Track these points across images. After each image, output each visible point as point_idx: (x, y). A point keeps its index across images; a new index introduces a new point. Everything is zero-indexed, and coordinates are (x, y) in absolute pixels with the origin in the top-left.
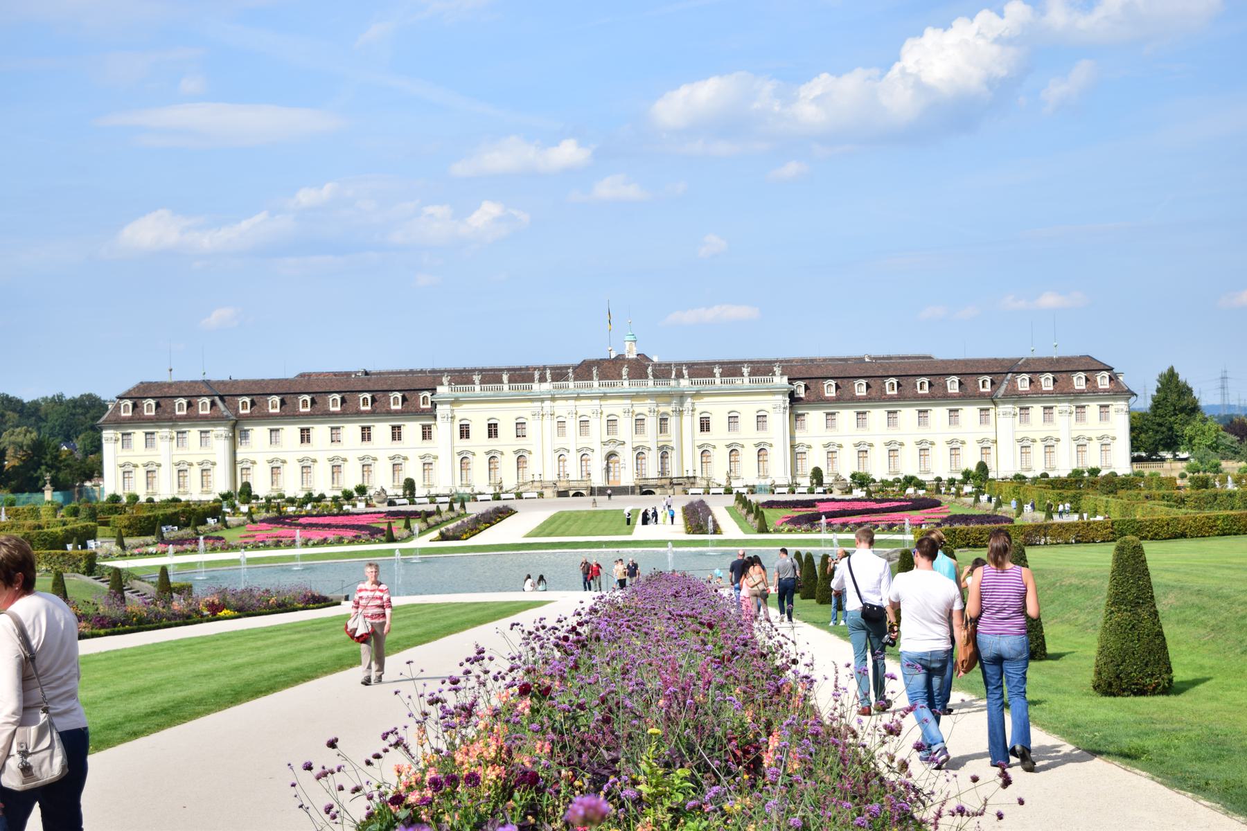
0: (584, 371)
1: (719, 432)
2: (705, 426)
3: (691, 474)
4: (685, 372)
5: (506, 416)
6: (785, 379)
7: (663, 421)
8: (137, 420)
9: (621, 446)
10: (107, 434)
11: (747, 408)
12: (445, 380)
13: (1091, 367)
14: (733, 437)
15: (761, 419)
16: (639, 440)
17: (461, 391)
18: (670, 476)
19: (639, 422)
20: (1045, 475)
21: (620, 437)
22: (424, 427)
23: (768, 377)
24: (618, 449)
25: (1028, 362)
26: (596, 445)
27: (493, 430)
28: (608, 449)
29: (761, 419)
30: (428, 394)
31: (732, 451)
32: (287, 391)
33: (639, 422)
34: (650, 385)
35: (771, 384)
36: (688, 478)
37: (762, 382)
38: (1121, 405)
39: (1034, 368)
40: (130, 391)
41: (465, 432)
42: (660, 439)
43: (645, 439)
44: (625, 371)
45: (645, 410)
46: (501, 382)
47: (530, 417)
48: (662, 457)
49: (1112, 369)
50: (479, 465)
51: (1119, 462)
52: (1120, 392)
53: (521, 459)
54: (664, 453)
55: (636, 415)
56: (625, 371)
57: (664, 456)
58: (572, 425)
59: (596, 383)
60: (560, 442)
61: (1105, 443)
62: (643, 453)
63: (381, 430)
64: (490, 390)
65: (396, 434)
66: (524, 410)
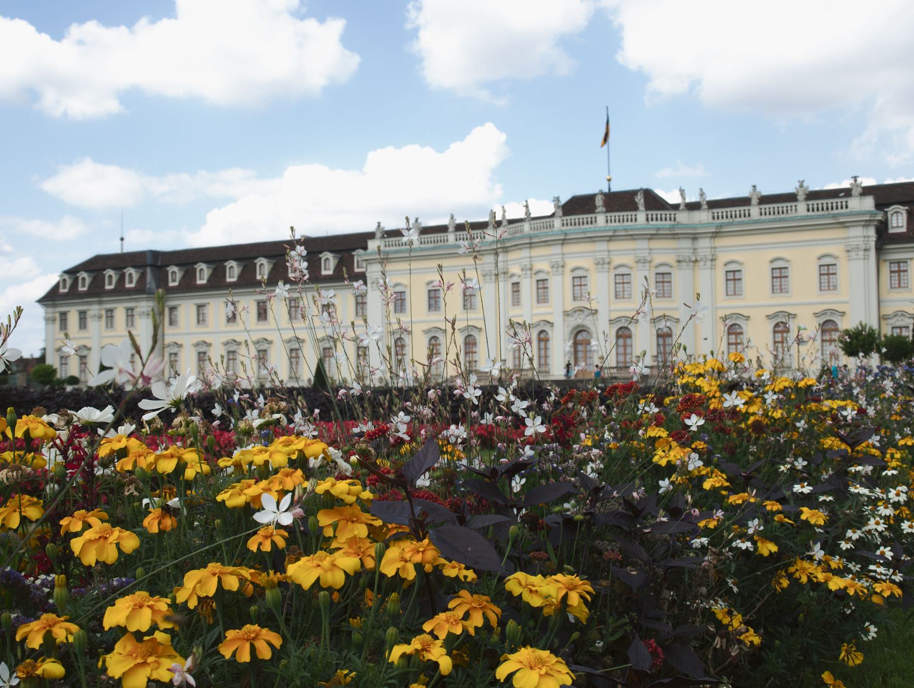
9: (591, 318)
21: (594, 306)
23: (839, 200)
24: (588, 322)
31: (777, 325)
33: (622, 280)
35: (844, 210)
42: (613, 307)
45: (628, 260)
58: (528, 287)
62: (627, 328)
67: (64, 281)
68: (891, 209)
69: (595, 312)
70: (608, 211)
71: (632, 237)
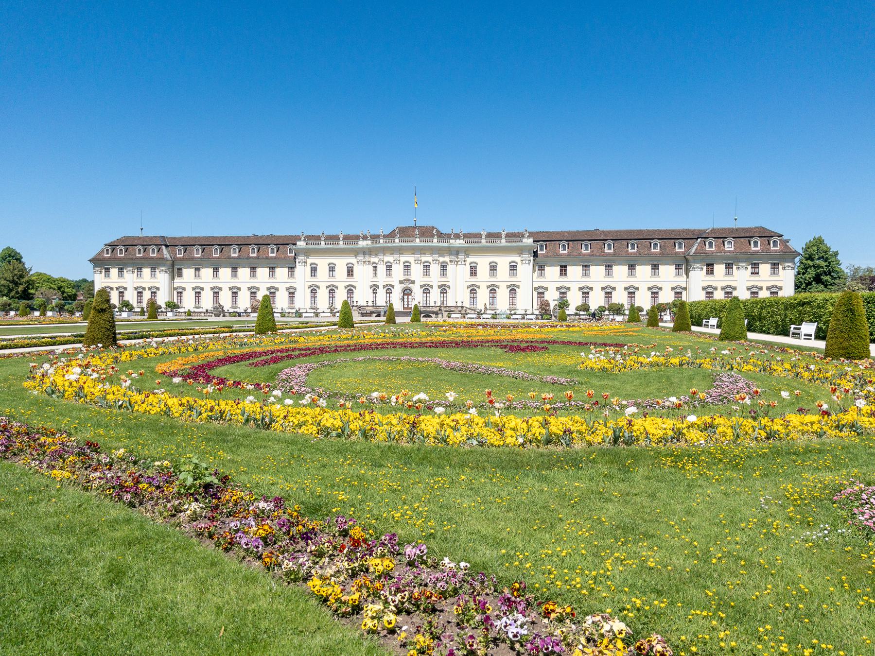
2: (473, 271)
6: (531, 240)
7: (444, 267)
11: (503, 262)
13: (767, 235)
16: (426, 280)
19: (427, 267)
21: (412, 278)
24: (411, 286)
28: (403, 286)
29: (513, 268)
30: (292, 247)
33: (427, 267)
36: (457, 307)
43: (429, 279)
49: (781, 236)
54: (444, 289)
55: (424, 263)
58: (382, 269)
67: (107, 250)
69: (413, 282)
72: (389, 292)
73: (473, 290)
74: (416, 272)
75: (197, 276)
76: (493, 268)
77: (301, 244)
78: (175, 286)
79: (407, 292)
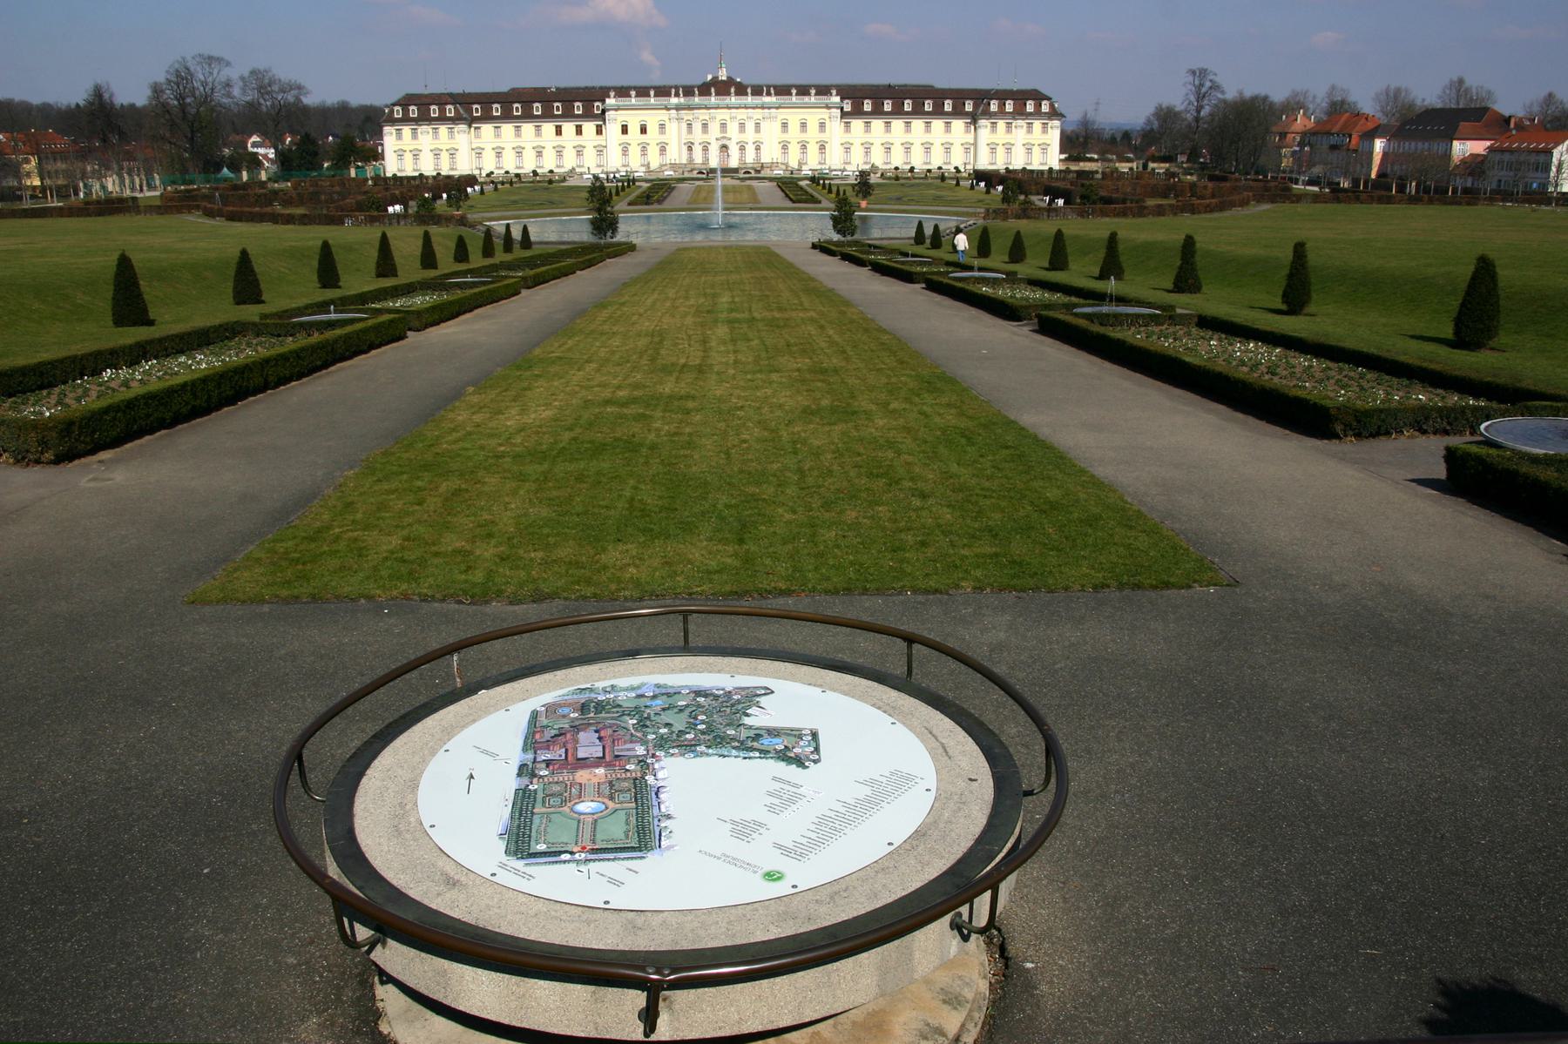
0: (704, 90)
1: (794, 131)
3: (775, 161)
4: (772, 92)
5: (653, 118)
7: (758, 125)
8: (406, 120)
10: (387, 129)
12: (612, 94)
13: (1038, 97)
14: (803, 137)
15: (822, 126)
16: (743, 137)
17: (623, 102)
18: (762, 161)
20: (1024, 169)
22: (597, 126)
25: (997, 92)
26: (713, 141)
27: (643, 130)
28: (720, 143)
29: (822, 126)
32: (506, 99)
33: (742, 126)
34: (749, 99)
37: (824, 99)
38: (1057, 123)
39: (1002, 96)
40: (399, 100)
41: (625, 130)
44: (733, 90)
46: (649, 96)
47: (667, 121)
48: (756, 149)
50: (635, 151)
51: (1052, 159)
52: (1054, 114)
53: (663, 150)
56: (733, 90)
57: (758, 149)
58: (697, 127)
59: (713, 99)
60: (690, 138)
61: (1044, 148)
63: (569, 127)
64: (642, 101)
65: (579, 131)
66: (662, 115)
68: (846, 101)
69: (730, 139)
70: (738, 93)
71: (746, 108)
72: (706, 149)
73: (785, 148)
74: (733, 128)
75: (498, 136)
76: (804, 125)
77: (610, 101)
78: (474, 146)
79: (724, 148)
